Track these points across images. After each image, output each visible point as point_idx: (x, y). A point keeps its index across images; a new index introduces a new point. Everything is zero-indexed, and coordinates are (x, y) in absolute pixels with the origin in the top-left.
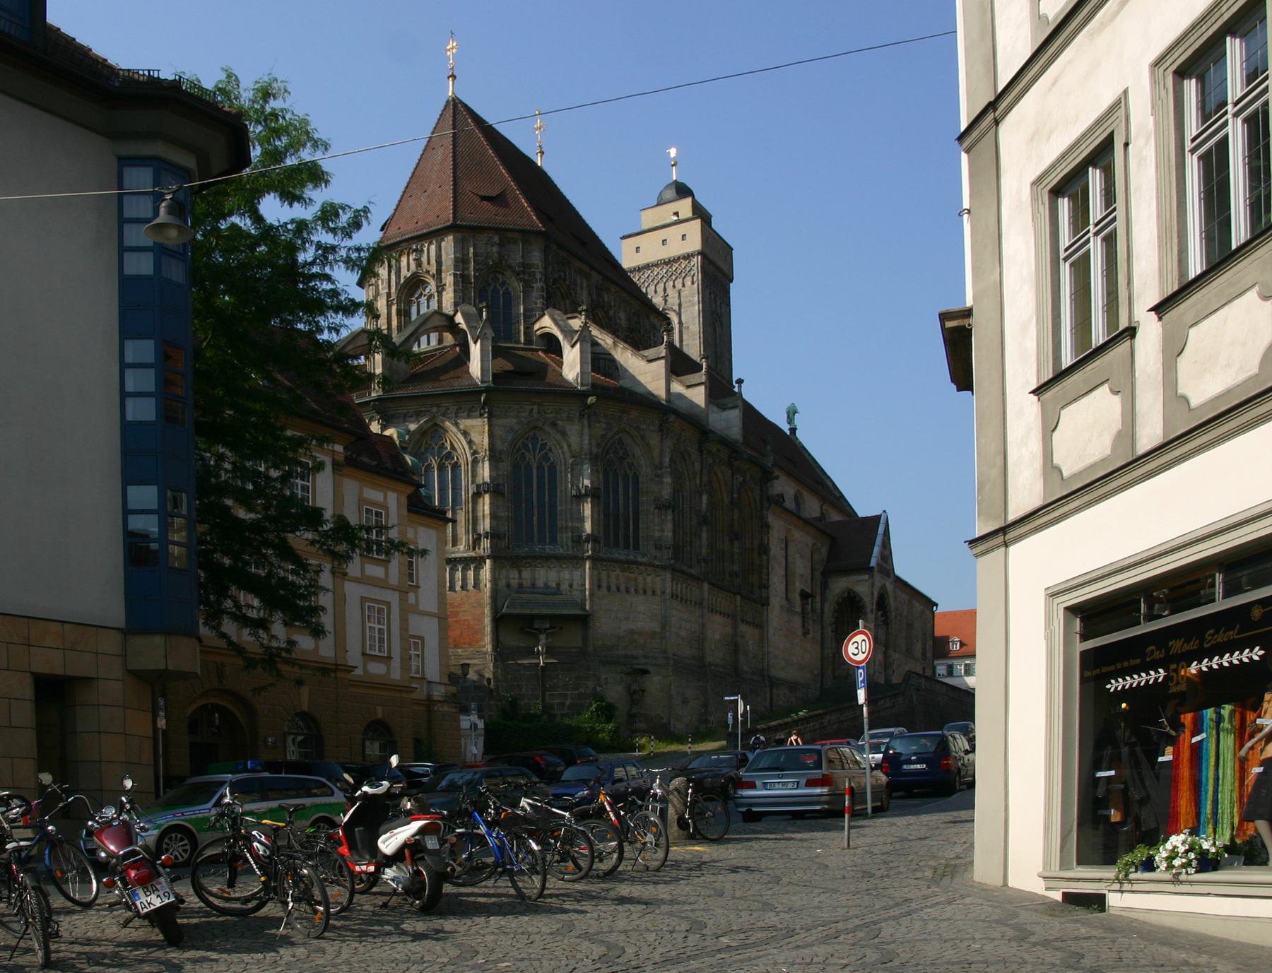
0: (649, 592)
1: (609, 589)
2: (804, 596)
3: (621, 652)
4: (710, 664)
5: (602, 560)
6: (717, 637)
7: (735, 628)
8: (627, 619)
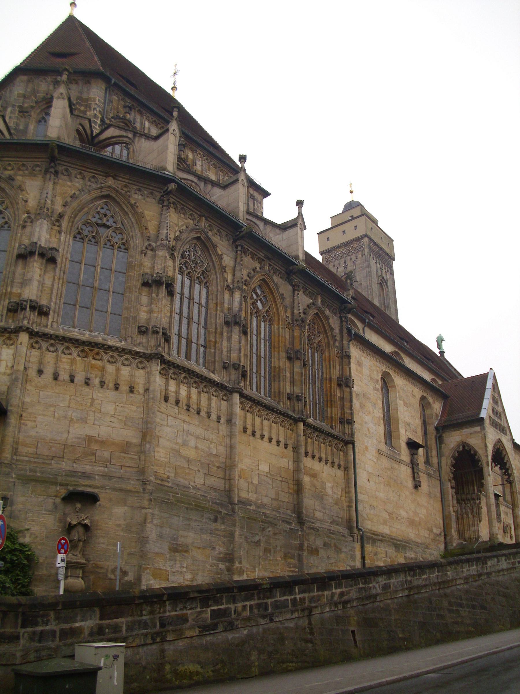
0: (124, 388)
1: (56, 377)
2: (412, 446)
3: (65, 465)
4: (244, 503)
5: (46, 336)
6: (264, 468)
7: (297, 461)
8: (84, 420)
